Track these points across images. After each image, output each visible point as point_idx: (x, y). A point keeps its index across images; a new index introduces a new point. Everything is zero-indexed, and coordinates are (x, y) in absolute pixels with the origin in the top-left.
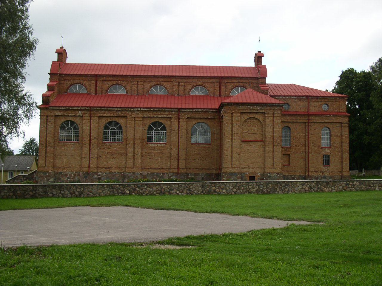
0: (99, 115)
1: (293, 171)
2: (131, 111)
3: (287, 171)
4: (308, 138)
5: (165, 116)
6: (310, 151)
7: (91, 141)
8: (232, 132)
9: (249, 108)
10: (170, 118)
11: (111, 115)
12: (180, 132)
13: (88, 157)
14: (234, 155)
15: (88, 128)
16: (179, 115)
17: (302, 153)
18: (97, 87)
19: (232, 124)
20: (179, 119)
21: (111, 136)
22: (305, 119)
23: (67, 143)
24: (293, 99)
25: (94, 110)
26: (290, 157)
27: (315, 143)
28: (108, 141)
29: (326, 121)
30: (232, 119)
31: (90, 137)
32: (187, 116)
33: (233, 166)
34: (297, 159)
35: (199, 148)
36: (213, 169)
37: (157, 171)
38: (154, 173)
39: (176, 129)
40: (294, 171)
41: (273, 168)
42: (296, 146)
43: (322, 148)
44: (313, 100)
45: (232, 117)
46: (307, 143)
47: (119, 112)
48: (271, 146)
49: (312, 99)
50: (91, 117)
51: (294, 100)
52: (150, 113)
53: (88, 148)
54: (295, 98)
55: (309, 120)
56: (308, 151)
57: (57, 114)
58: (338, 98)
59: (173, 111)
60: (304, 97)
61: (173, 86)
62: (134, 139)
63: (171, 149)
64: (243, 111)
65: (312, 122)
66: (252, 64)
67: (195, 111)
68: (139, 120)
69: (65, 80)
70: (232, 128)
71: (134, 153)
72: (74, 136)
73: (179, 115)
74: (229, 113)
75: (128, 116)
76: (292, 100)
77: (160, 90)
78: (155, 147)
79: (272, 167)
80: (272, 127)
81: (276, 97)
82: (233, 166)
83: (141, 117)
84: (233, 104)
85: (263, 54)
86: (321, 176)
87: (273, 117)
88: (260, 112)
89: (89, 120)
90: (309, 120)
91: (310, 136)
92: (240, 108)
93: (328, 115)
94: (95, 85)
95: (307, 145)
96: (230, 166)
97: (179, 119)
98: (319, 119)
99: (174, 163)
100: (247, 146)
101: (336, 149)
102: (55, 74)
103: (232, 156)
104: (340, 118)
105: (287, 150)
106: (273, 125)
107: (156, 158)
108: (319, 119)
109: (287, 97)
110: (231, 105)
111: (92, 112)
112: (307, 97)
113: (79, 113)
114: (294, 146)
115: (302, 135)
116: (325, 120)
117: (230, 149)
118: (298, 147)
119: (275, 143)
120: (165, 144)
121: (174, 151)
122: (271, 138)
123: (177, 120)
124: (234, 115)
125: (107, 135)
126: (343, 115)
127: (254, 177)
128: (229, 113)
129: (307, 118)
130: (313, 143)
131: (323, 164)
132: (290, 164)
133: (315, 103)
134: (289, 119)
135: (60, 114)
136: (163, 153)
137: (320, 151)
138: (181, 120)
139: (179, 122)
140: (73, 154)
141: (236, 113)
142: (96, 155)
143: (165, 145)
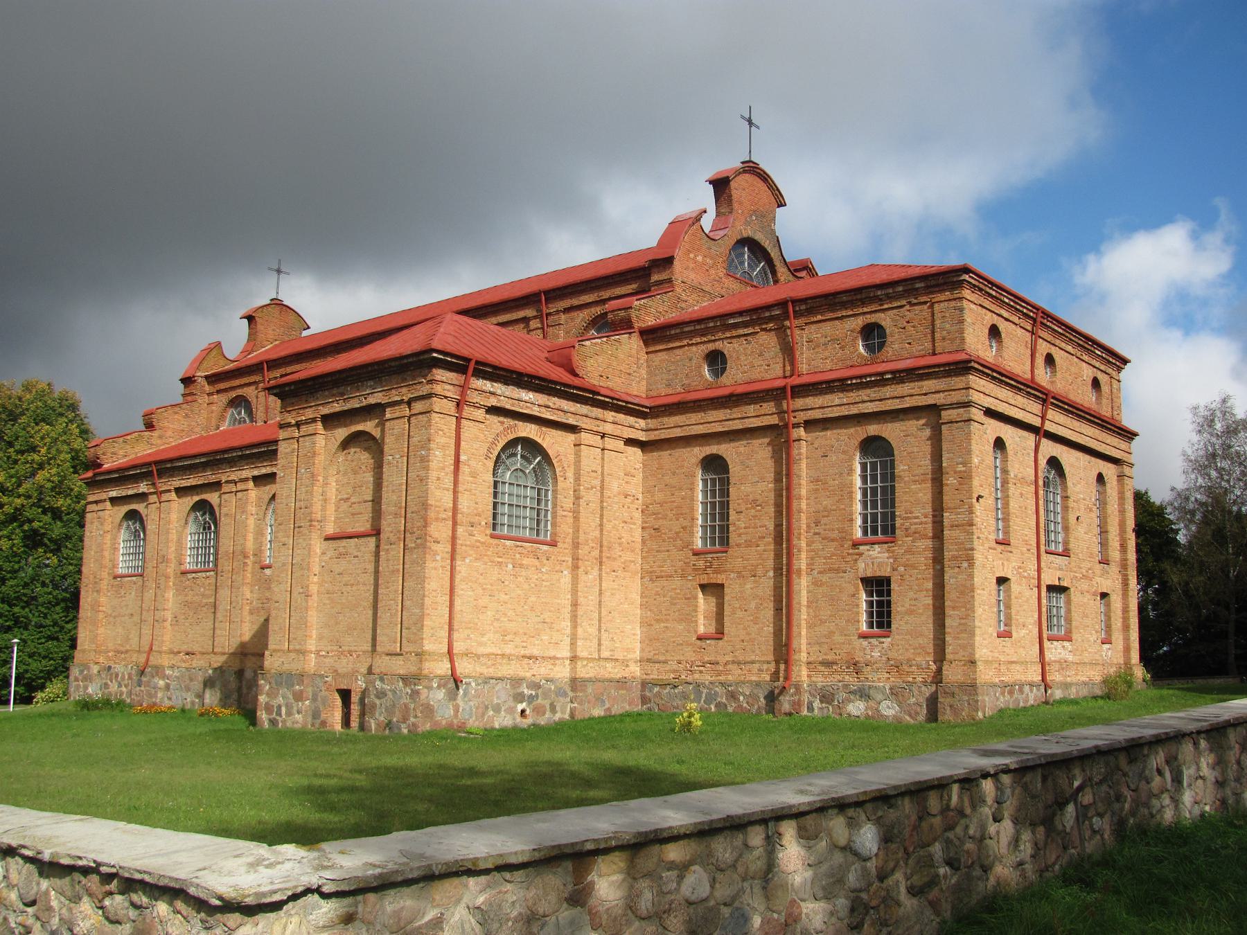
1: (733, 662)
26: (726, 598)
27: (824, 521)
34: (753, 605)
40: (739, 663)
42: (749, 544)
54: (740, 320)
76: (734, 333)
81: (673, 332)
84: (293, 388)
86: (846, 686)
93: (870, 375)
104: (929, 385)
105: (715, 563)
108: (837, 402)
109: (711, 324)
113: (143, 487)
114: (738, 545)
116: (864, 402)
118: (758, 546)
126: (938, 366)
132: (726, 631)
137: (849, 558)
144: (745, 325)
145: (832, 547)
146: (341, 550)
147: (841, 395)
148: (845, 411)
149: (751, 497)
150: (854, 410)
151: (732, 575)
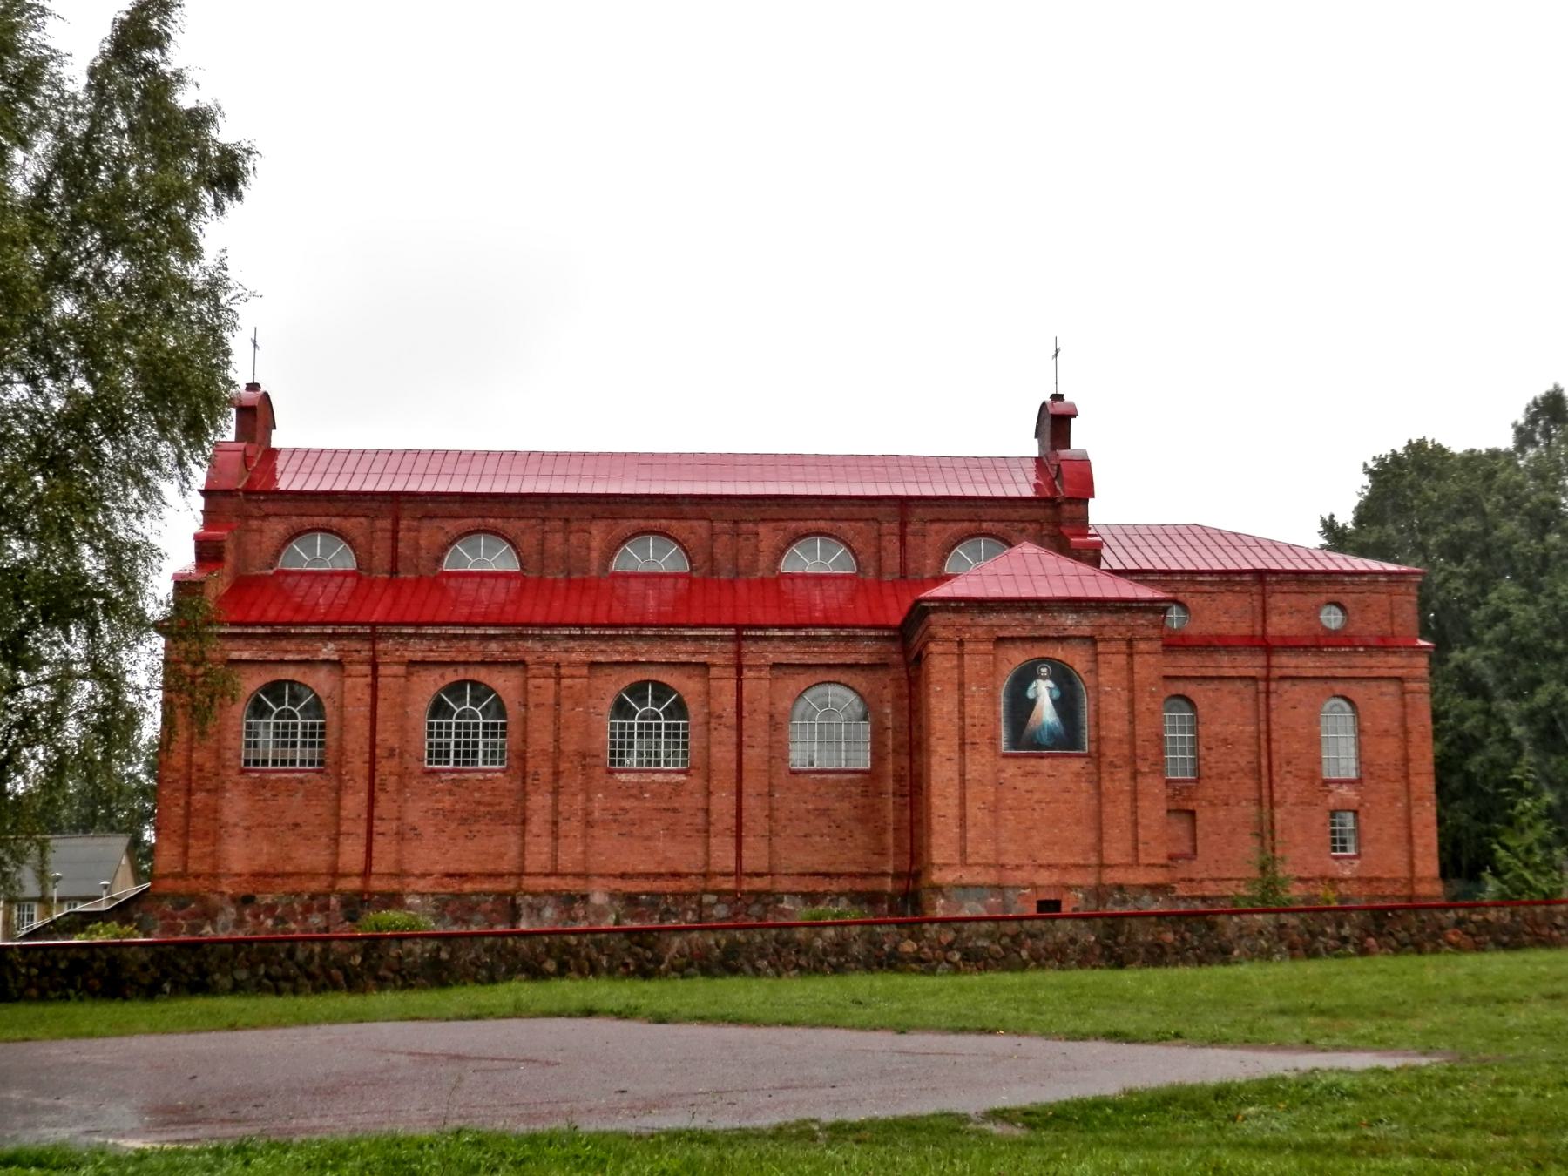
0: (409, 655)
2: (541, 638)
3: (1183, 880)
4: (1269, 741)
5: (683, 658)
6: (1277, 796)
7: (377, 767)
8: (962, 717)
9: (1028, 620)
10: (706, 666)
11: (462, 658)
12: (746, 723)
13: (362, 830)
14: (973, 810)
15: (365, 710)
16: (739, 654)
17: (1244, 803)
18: (401, 545)
19: (961, 685)
20: (739, 669)
21: (457, 744)
22: (1251, 664)
23: (273, 777)
24: (1202, 583)
25: (390, 636)
26: (1198, 823)
28: (447, 763)
29: (1340, 672)
30: (961, 666)
31: (373, 746)
32: (771, 658)
33: (970, 861)
34: (1227, 829)
35: (823, 790)
36: (884, 874)
37: (647, 886)
38: (639, 894)
39: (730, 710)
41: (1136, 863)
42: (1220, 776)
43: (1326, 783)
44: (1285, 589)
45: (961, 656)
46: (1264, 762)
47: (493, 646)
48: (1123, 774)
49: (1278, 583)
50: (375, 666)
51: (1207, 588)
52: (621, 648)
53: (363, 795)
55: (1269, 667)
56: (1271, 797)
57: (235, 655)
58: (1382, 579)
59: (713, 638)
60: (1247, 578)
61: (713, 534)
62: (558, 751)
63: (709, 794)
64: (1005, 633)
65: (1283, 678)
66: (1032, 448)
67: (807, 638)
68: (572, 677)
69: (266, 516)
70: (962, 703)
71: (556, 811)
72: (304, 744)
73: (739, 654)
74: (947, 640)
75: (529, 659)
76: (1199, 588)
77: (658, 557)
78: (642, 788)
79: (1129, 860)
80: (1125, 695)
82: (970, 861)
83: (583, 664)
84: (963, 604)
85: (1073, 406)
87: (1131, 655)
88: (1075, 637)
89: (369, 679)
90: (1269, 667)
91: (1274, 736)
92: (994, 619)
94: (388, 535)
95: (1264, 771)
96: (957, 859)
97: (739, 669)
98: (1309, 664)
99: (723, 856)
100: (1027, 774)
101: (1384, 786)
102: (229, 493)
103: (962, 819)
105: (1185, 793)
106: (1131, 690)
107: (647, 831)
108: (1311, 664)
109: (1179, 578)
110: (957, 610)
111: (381, 646)
112: (1260, 575)
115: (1242, 732)
117: (953, 791)
119: (1139, 763)
120: (685, 772)
121: (723, 802)
122: (1120, 741)
123: (732, 672)
124: (969, 647)
125: (443, 740)
127: (1056, 905)
128: (947, 640)
129: (1260, 660)
130: (1289, 763)
131: (1334, 849)
133: (1293, 599)
134: (1188, 664)
135: (246, 655)
136: (675, 810)
138: (747, 673)
139: (739, 679)
140: (299, 820)
141: (977, 640)
142: (394, 825)
143: (682, 778)
144: (1212, 584)
145: (1303, 785)
146: (1029, 769)
147: (1314, 659)
148: (1318, 673)
149: (1221, 737)
150: (1327, 673)
151: (1204, 803)
